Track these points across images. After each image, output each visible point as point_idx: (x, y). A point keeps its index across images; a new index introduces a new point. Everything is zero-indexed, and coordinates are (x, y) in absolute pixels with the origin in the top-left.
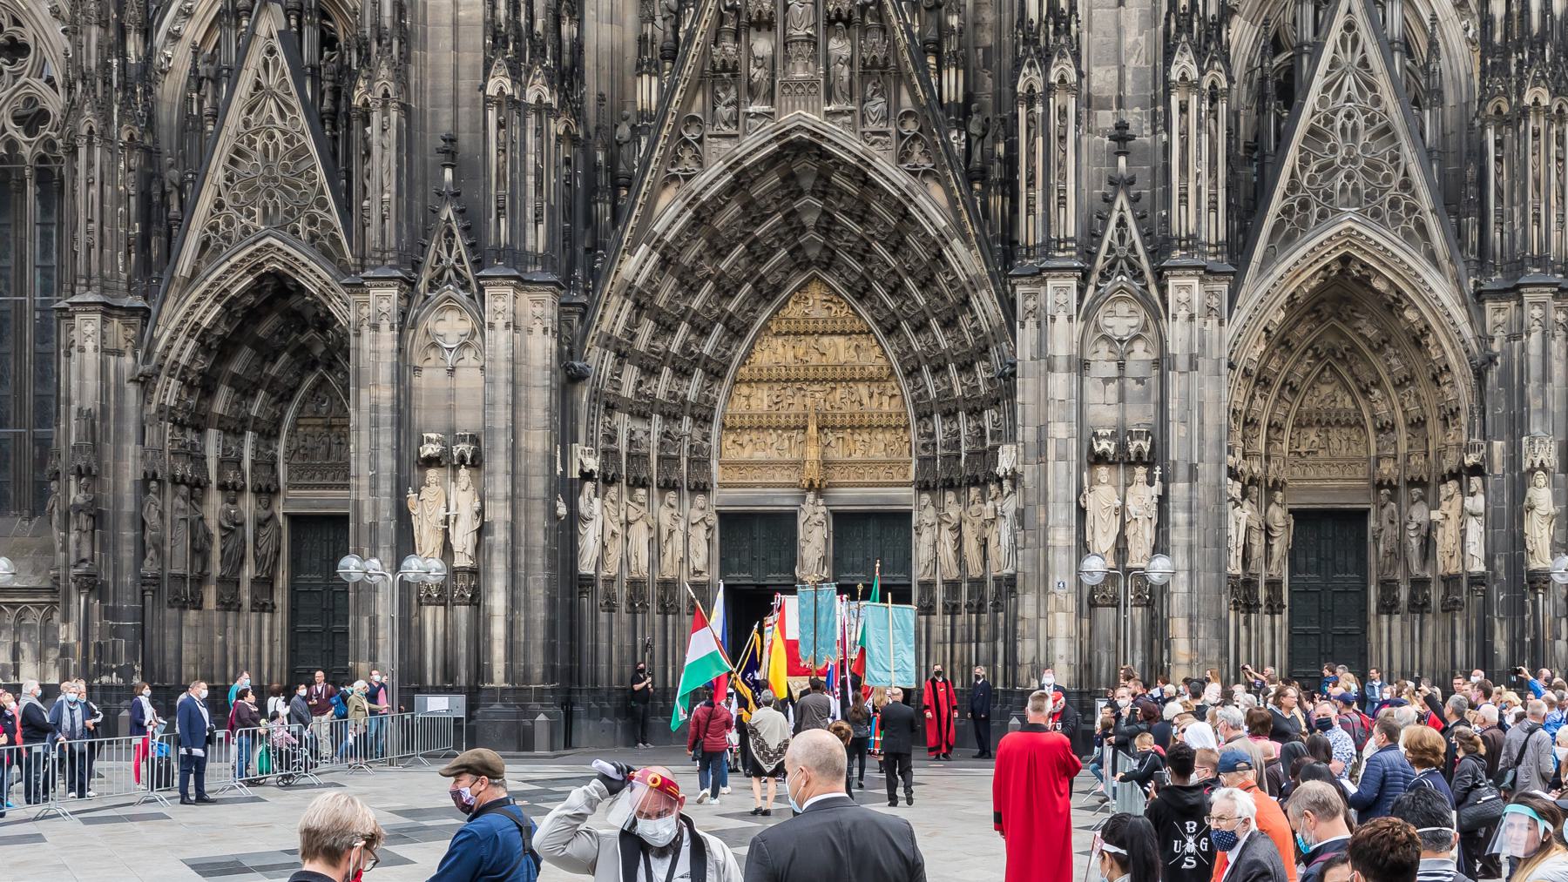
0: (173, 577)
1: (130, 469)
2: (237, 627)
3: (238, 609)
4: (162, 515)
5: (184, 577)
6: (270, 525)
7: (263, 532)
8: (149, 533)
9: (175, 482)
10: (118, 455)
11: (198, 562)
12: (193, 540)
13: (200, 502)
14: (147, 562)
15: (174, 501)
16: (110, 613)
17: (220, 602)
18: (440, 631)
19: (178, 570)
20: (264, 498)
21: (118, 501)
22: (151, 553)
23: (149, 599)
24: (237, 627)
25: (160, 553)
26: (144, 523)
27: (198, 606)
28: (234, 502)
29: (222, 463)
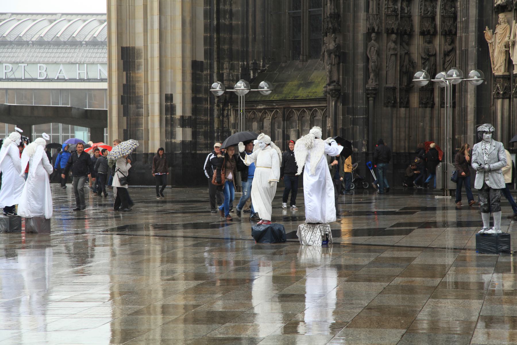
0: (387, 89)
1: (362, 27)
2: (432, 118)
3: (433, 106)
4: (378, 53)
5: (394, 89)
6: (452, 55)
7: (448, 59)
8: (371, 64)
9: (390, 32)
10: (355, 18)
11: (405, 79)
12: (401, 66)
13: (408, 44)
14: (370, 81)
15: (389, 45)
16: (347, 111)
17: (421, 103)
18: (506, 114)
19: (390, 85)
20: (449, 38)
21: (355, 46)
22: (372, 75)
23: (371, 102)
24: (432, 118)
25: (377, 75)
26: (368, 59)
27: (407, 105)
28: (430, 42)
29: (423, 18)
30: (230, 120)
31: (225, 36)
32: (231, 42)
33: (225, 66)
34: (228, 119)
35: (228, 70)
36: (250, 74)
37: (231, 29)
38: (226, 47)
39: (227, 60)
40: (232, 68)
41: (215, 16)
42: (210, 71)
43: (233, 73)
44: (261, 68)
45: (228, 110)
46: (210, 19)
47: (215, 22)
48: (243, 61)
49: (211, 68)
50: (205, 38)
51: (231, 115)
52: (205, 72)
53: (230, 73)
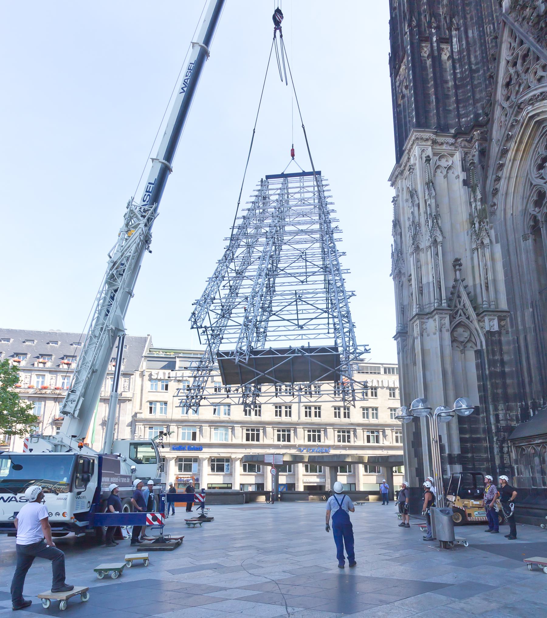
30: (511, 456)
31: (497, 381)
32: (505, 386)
33: (500, 408)
34: (509, 455)
35: (504, 411)
36: (530, 413)
37: (503, 375)
38: (500, 391)
39: (502, 402)
40: (508, 409)
41: (487, 367)
42: (486, 414)
43: (511, 414)
44: (542, 406)
45: (508, 447)
46: (482, 369)
47: (487, 372)
48: (521, 402)
49: (487, 410)
50: (479, 387)
51: (512, 452)
52: (481, 415)
53: (506, 414)
